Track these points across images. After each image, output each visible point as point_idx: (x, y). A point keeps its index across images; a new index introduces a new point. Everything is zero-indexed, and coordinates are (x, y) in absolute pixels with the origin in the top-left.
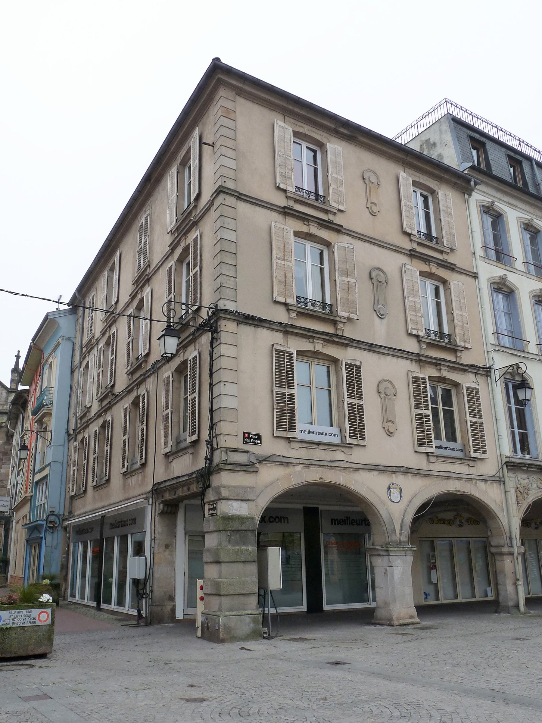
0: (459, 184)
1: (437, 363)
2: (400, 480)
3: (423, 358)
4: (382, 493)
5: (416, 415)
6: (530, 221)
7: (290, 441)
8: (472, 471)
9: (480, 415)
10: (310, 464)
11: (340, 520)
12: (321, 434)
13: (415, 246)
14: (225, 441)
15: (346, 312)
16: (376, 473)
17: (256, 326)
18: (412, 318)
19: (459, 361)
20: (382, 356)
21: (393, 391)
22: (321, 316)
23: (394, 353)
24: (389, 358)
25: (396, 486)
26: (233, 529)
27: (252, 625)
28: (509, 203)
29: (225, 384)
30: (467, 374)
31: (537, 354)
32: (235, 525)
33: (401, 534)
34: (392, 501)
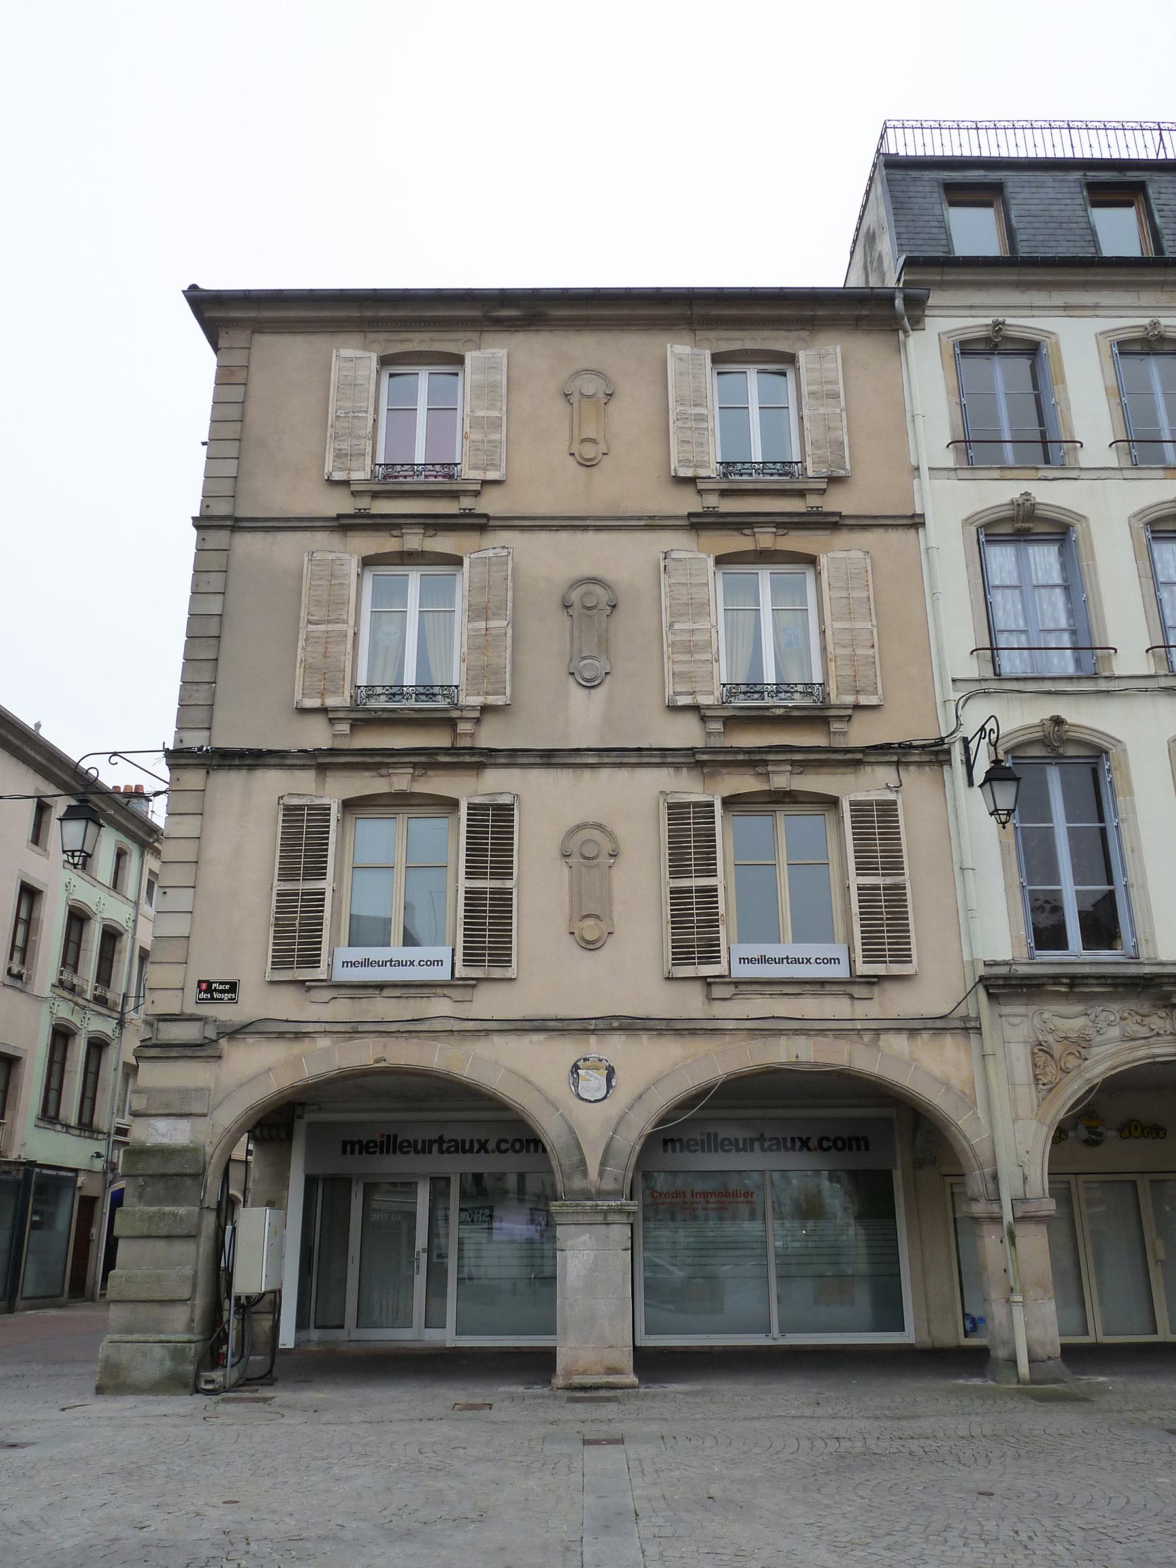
0: (866, 316)
1: (754, 760)
2: (615, 1048)
3: (705, 757)
4: (555, 1081)
5: (859, 889)
6: (1149, 328)
7: (309, 989)
8: (863, 1009)
9: (894, 866)
10: (354, 1031)
11: (368, 1142)
12: (796, 961)
13: (712, 501)
14: (153, 1002)
15: (478, 695)
16: (541, 1037)
17: (251, 767)
18: (678, 668)
19: (839, 742)
20: (587, 774)
21: (607, 847)
22: (409, 716)
23: (618, 760)
24: (605, 773)
25: (599, 1064)
26: (150, 1172)
27: (168, 1363)
28: (1065, 307)
29: (165, 893)
30: (868, 769)
31: (1152, 672)
32: (154, 1166)
33: (601, 1174)
34: (583, 1099)
